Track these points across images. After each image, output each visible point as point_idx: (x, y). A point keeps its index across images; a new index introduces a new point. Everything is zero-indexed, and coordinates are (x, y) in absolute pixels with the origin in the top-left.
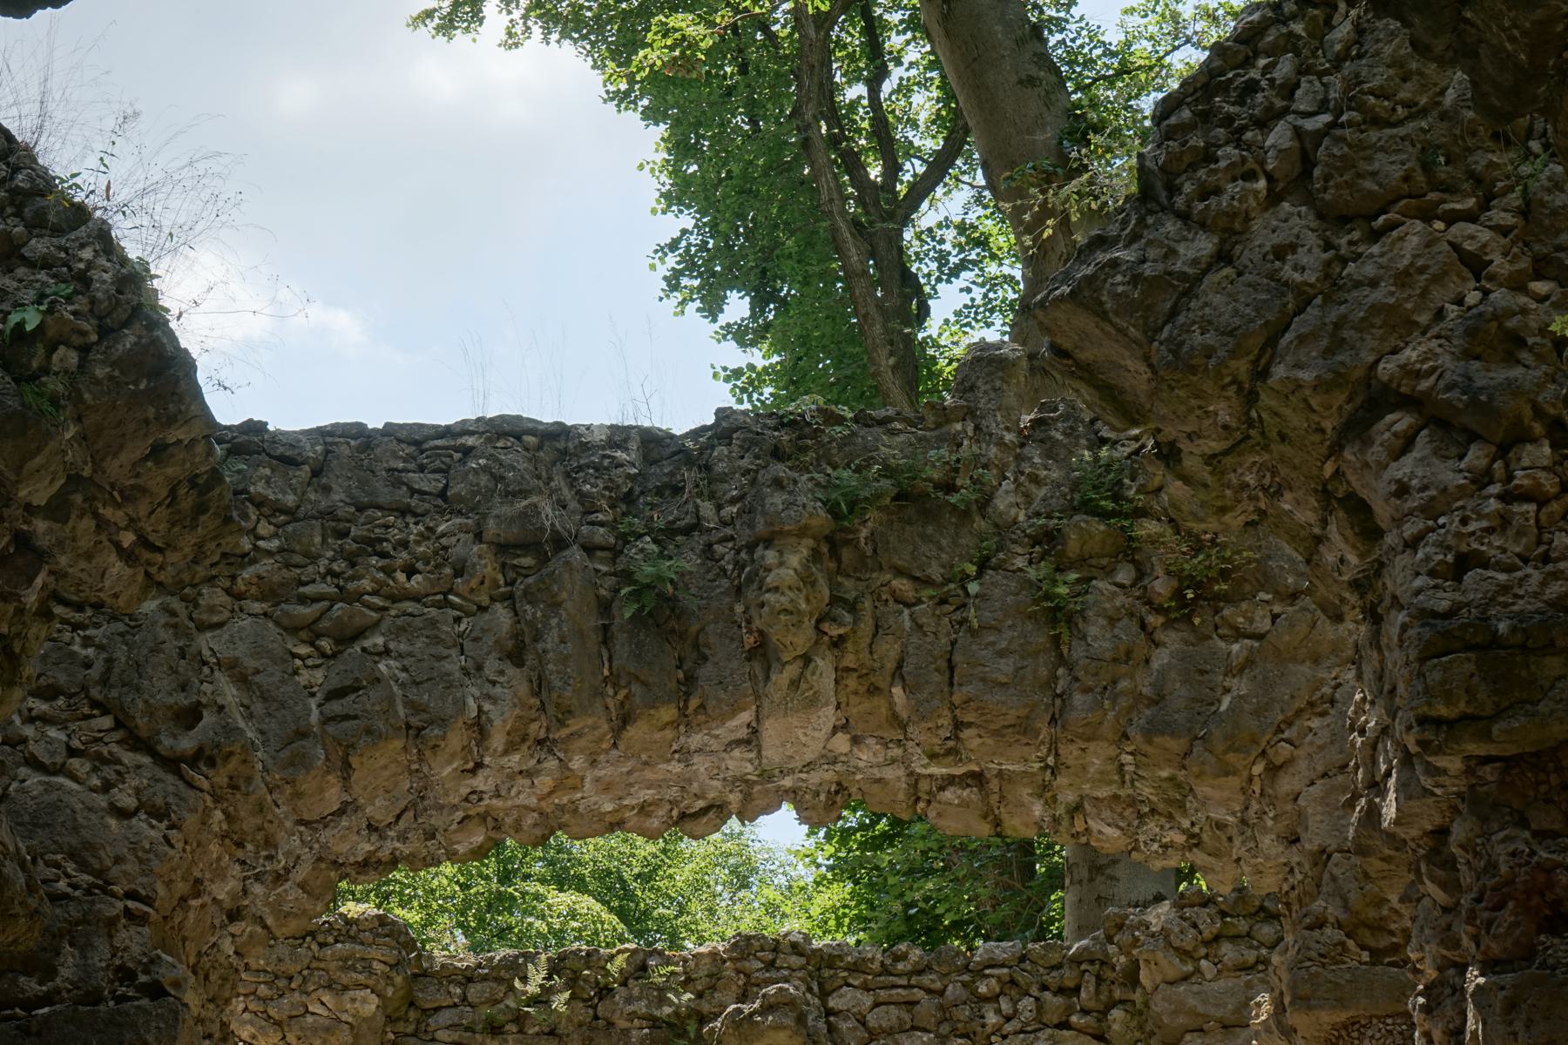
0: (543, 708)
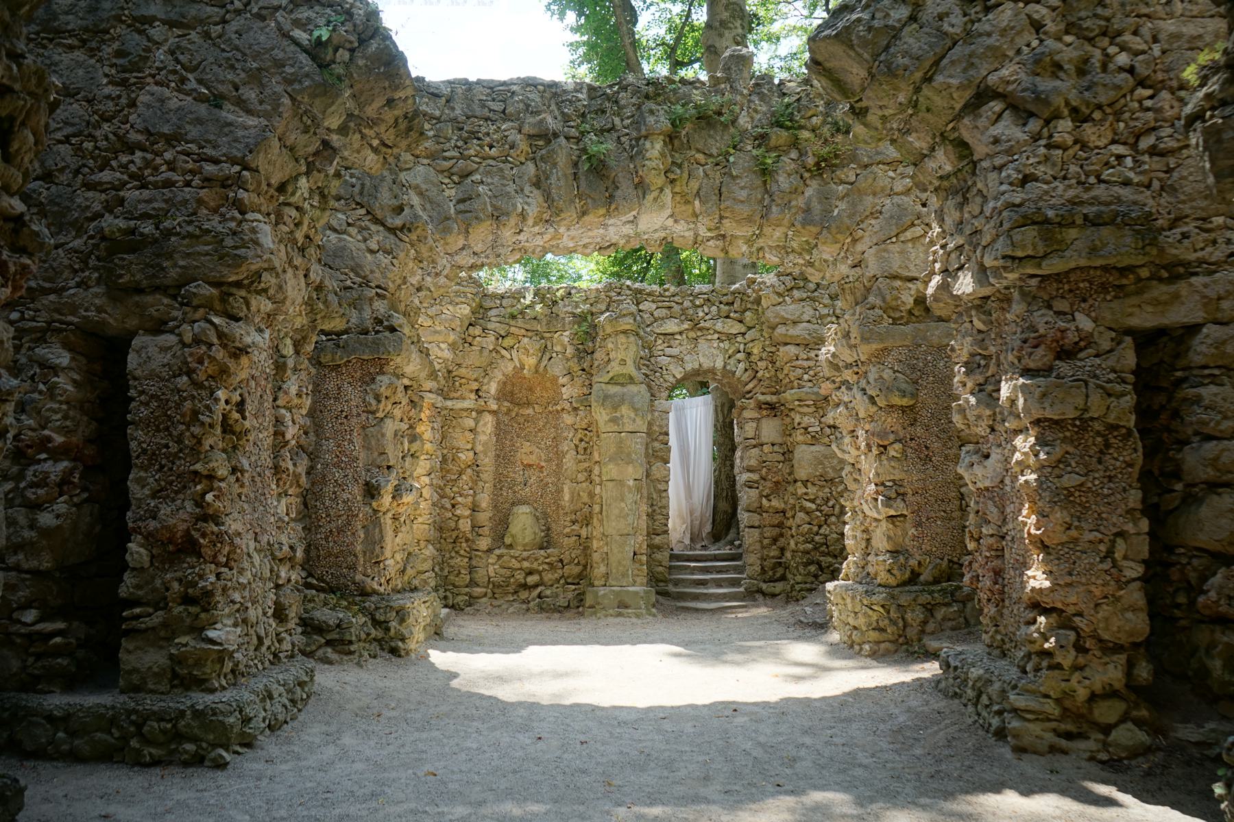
0: (549, 207)
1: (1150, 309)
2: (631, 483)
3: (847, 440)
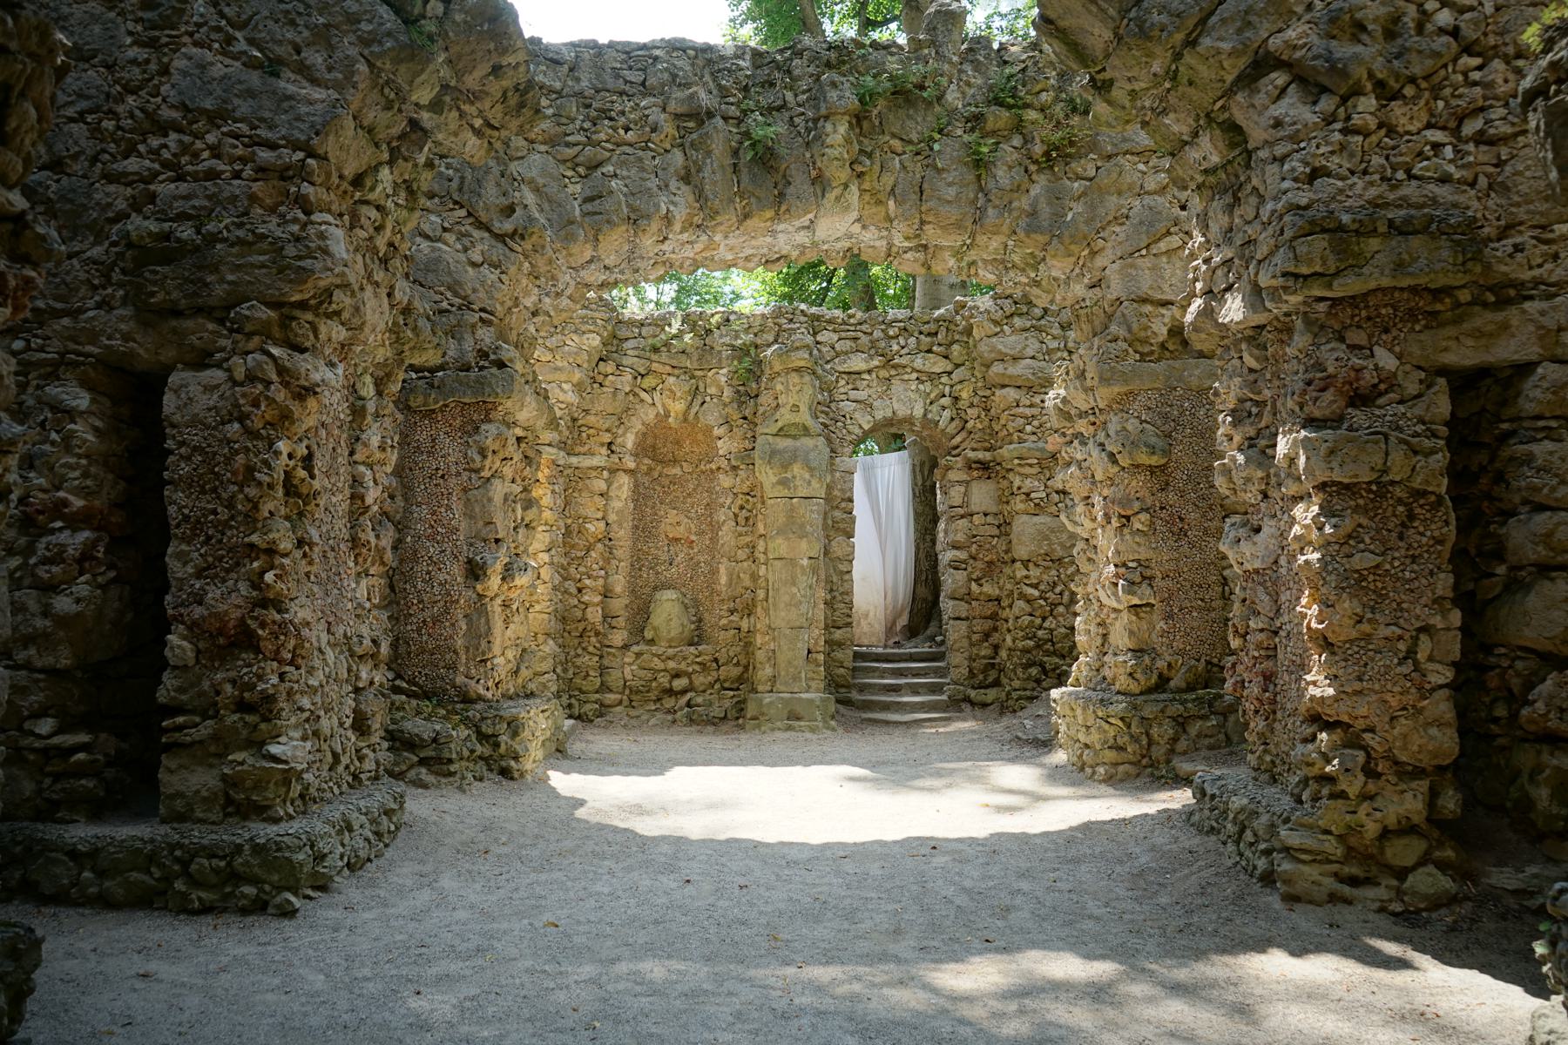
0: (701, 208)
1: (1470, 342)
2: (805, 562)
3: (1080, 509)
